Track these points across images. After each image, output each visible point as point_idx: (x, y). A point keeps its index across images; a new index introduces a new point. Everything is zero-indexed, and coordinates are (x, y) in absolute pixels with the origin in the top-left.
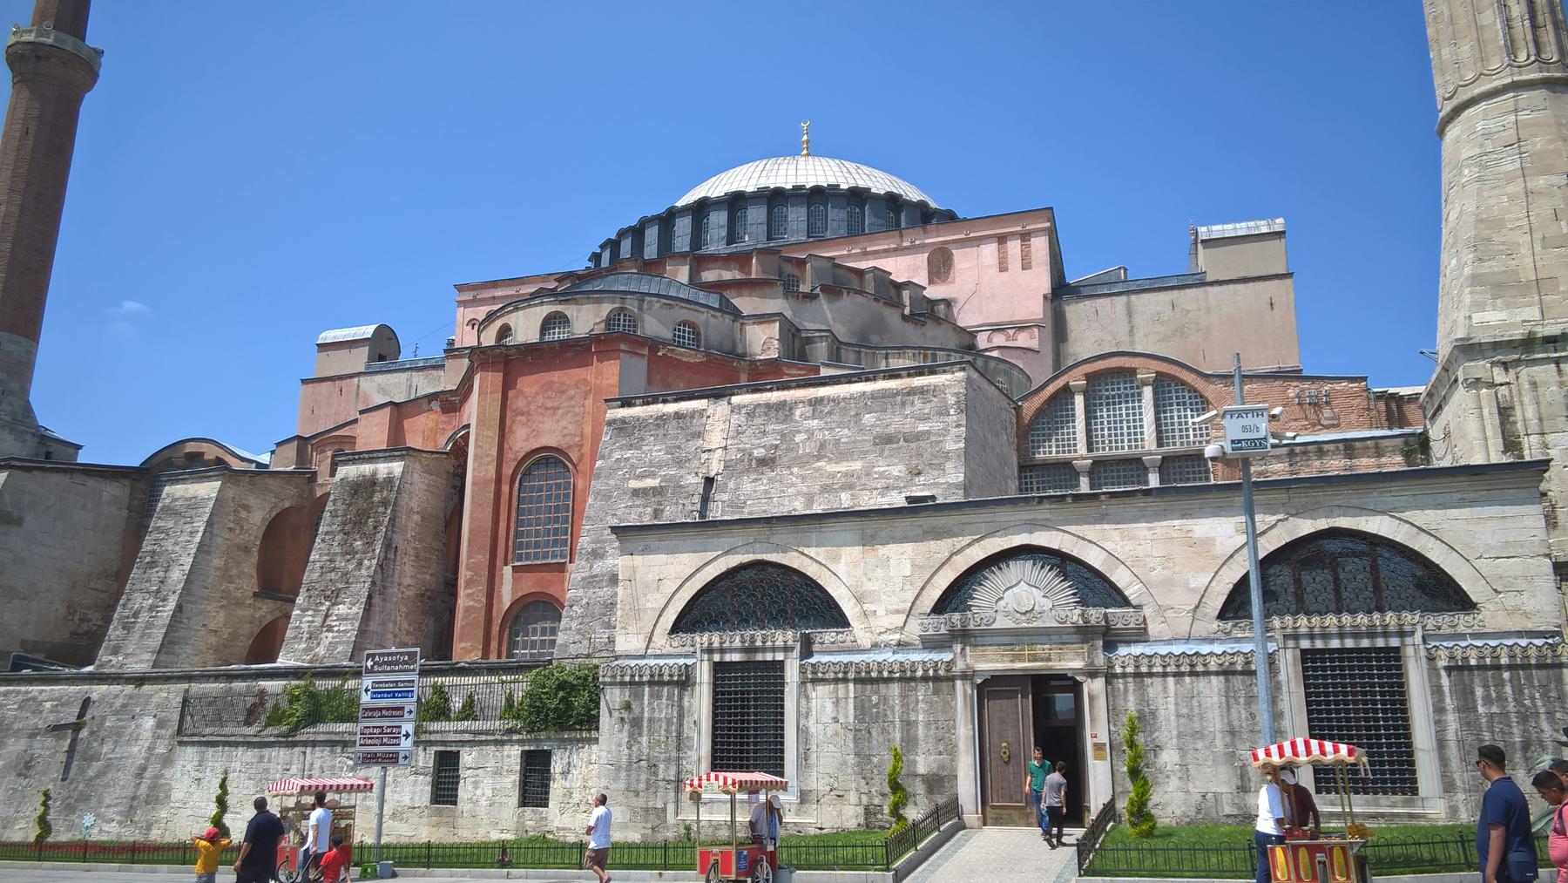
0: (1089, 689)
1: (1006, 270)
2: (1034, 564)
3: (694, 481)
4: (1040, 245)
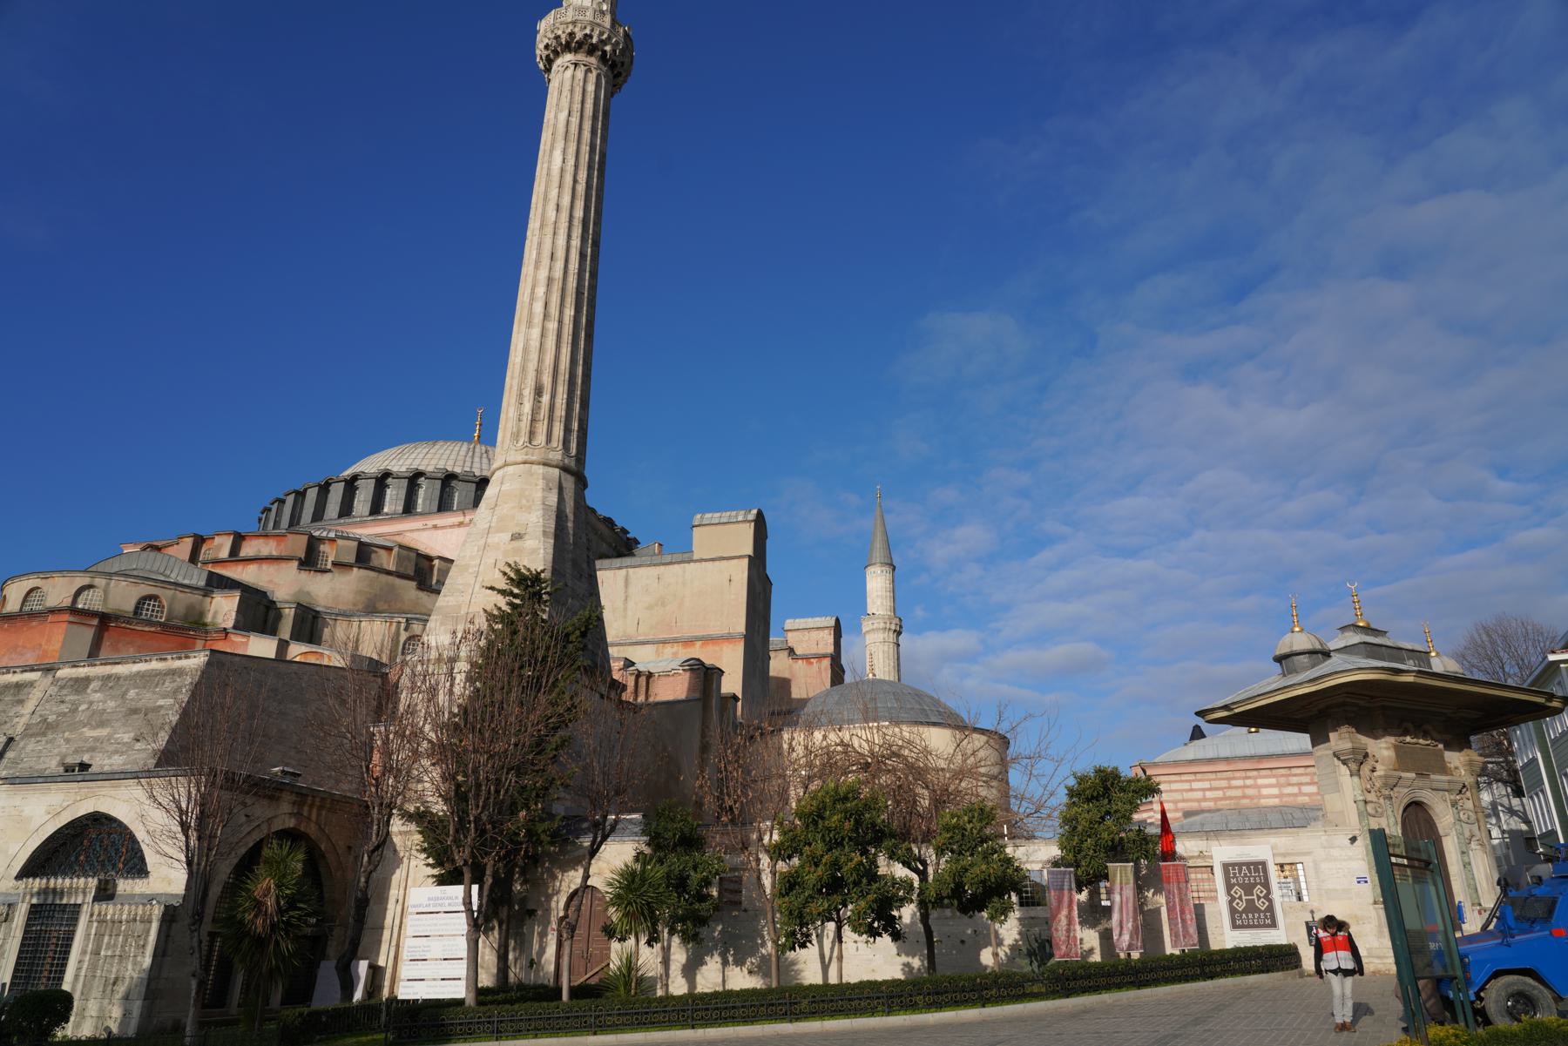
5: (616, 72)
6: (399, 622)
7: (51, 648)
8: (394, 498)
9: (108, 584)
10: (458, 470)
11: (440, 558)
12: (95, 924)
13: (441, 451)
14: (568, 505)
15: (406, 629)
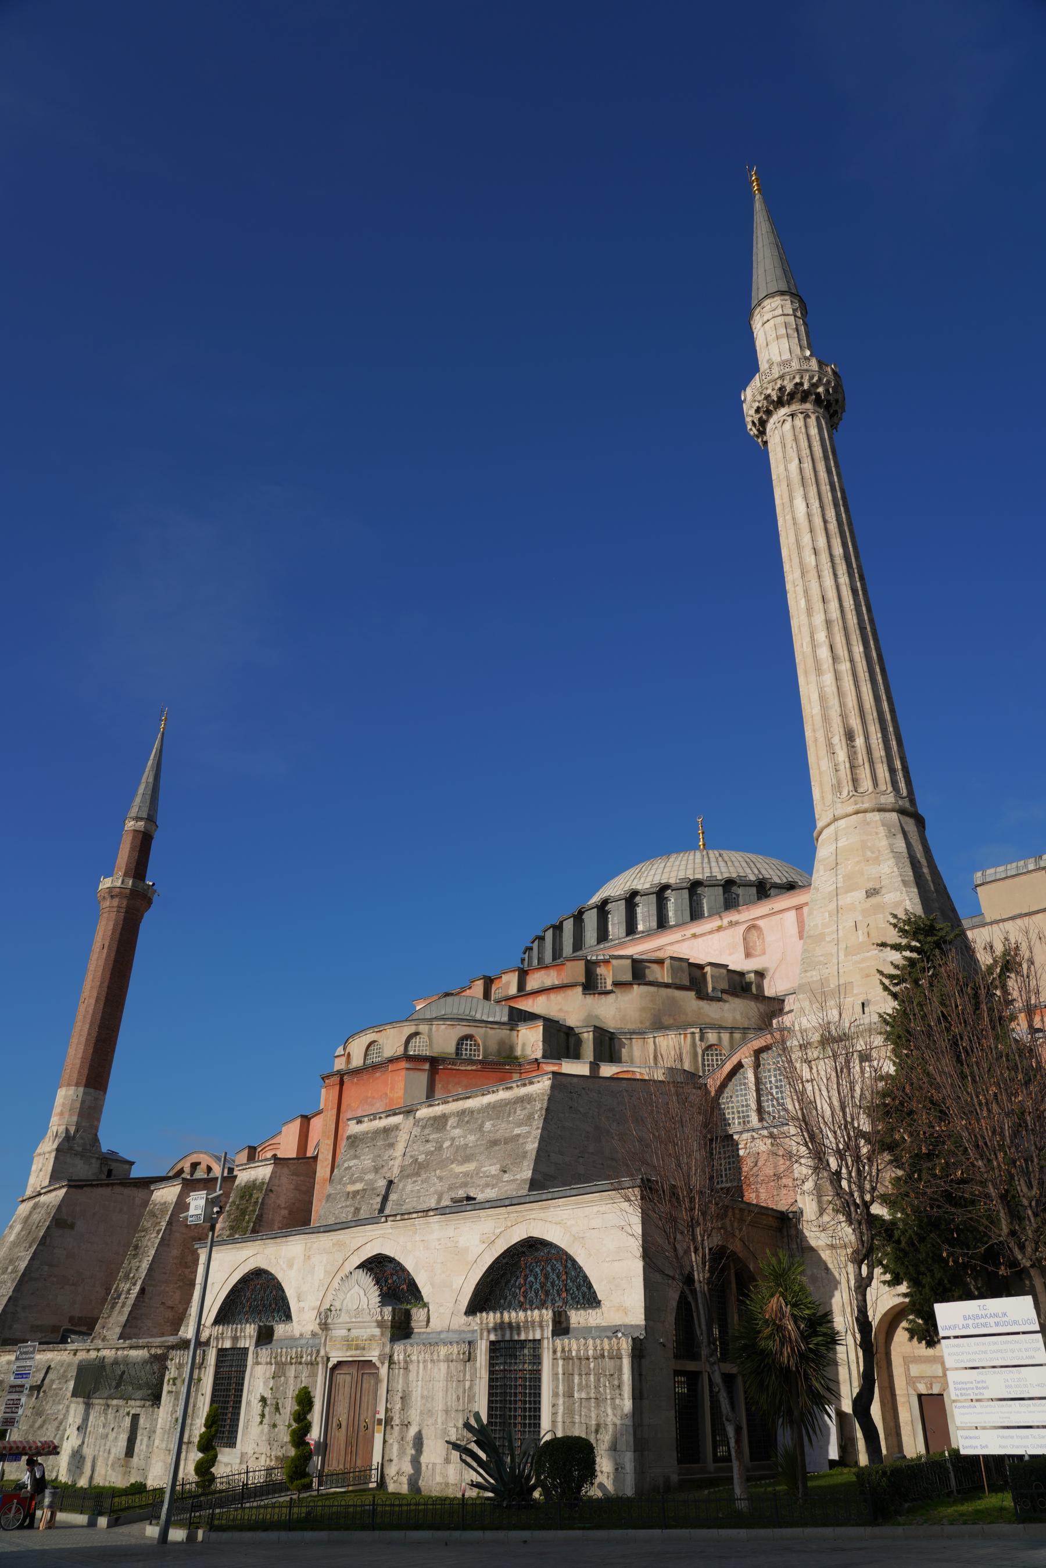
3: (382, 1183)
5: (832, 411)
6: (693, 1033)
7: (396, 1095)
8: (616, 925)
9: (430, 1030)
10: (699, 876)
11: (711, 964)
12: (561, 1362)
13: (677, 863)
14: (917, 851)
15: (702, 1039)
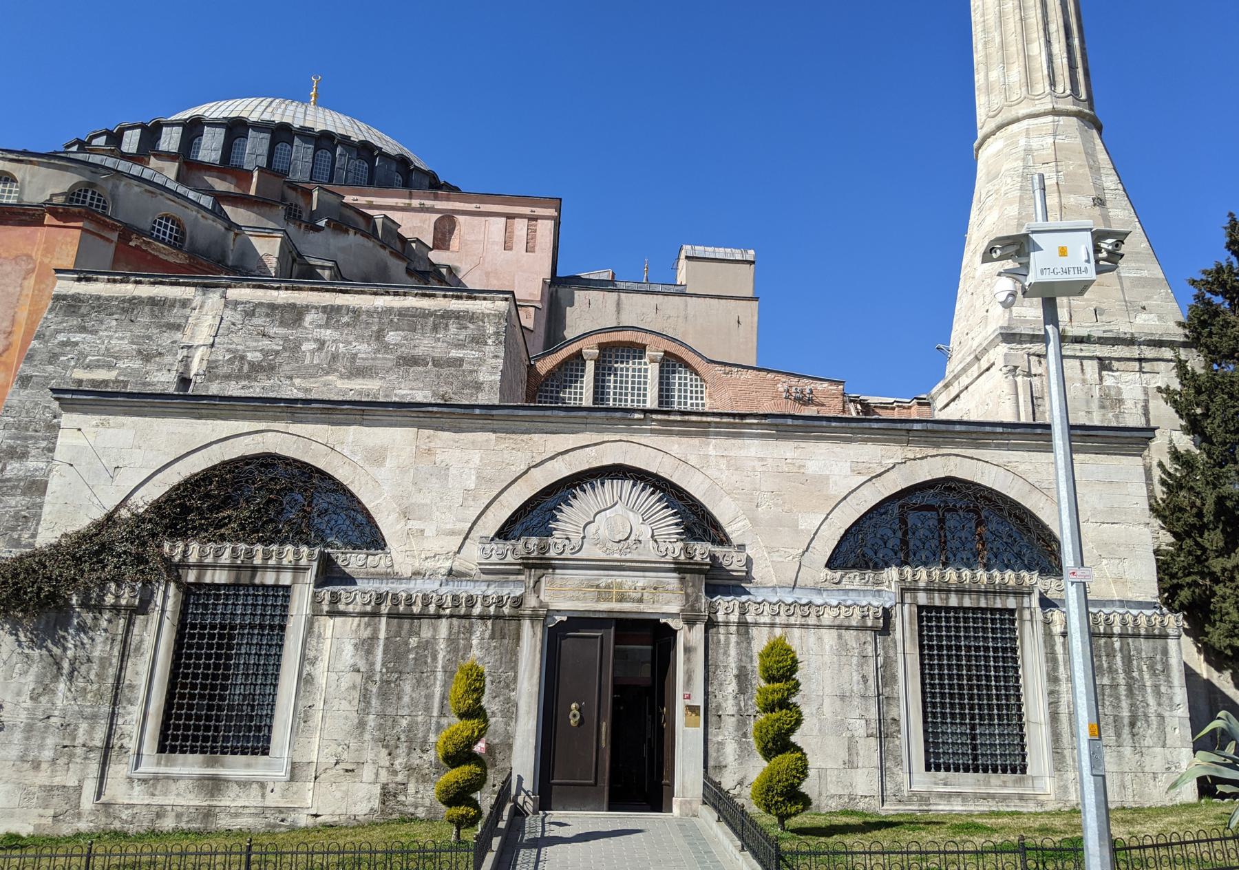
0: (685, 638)
1: (511, 249)
2: (634, 485)
4: (545, 229)
